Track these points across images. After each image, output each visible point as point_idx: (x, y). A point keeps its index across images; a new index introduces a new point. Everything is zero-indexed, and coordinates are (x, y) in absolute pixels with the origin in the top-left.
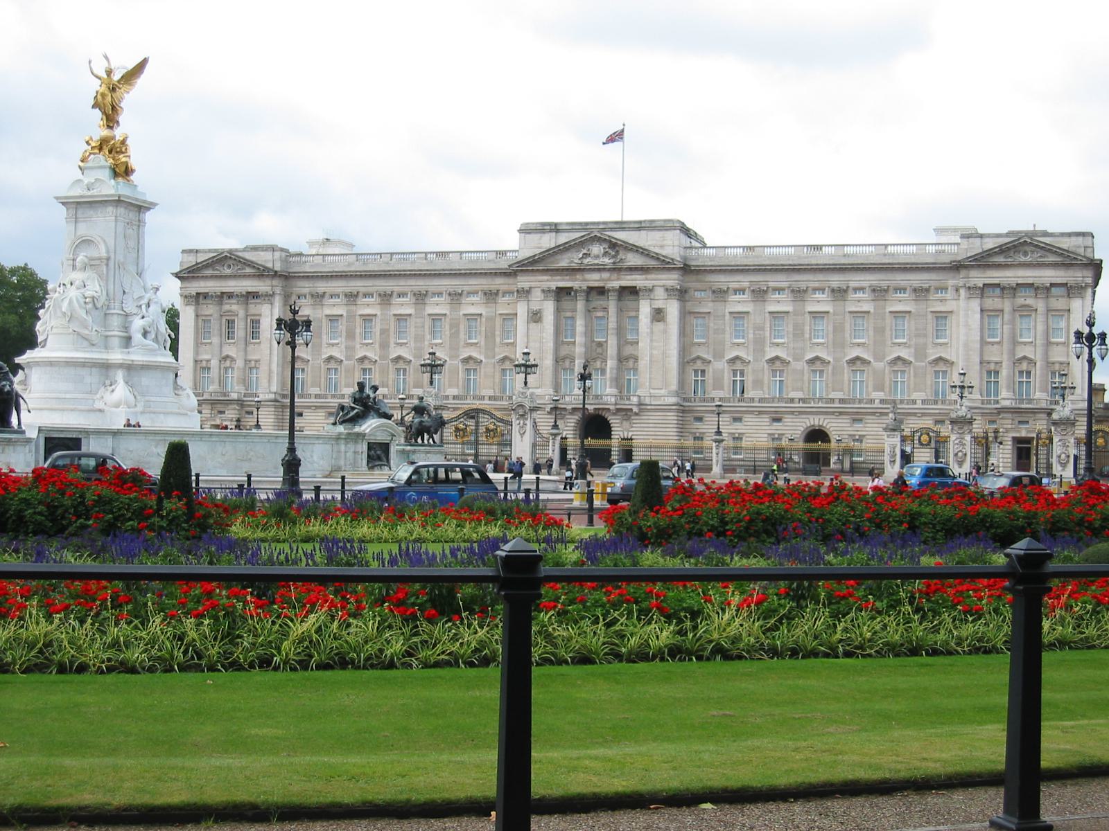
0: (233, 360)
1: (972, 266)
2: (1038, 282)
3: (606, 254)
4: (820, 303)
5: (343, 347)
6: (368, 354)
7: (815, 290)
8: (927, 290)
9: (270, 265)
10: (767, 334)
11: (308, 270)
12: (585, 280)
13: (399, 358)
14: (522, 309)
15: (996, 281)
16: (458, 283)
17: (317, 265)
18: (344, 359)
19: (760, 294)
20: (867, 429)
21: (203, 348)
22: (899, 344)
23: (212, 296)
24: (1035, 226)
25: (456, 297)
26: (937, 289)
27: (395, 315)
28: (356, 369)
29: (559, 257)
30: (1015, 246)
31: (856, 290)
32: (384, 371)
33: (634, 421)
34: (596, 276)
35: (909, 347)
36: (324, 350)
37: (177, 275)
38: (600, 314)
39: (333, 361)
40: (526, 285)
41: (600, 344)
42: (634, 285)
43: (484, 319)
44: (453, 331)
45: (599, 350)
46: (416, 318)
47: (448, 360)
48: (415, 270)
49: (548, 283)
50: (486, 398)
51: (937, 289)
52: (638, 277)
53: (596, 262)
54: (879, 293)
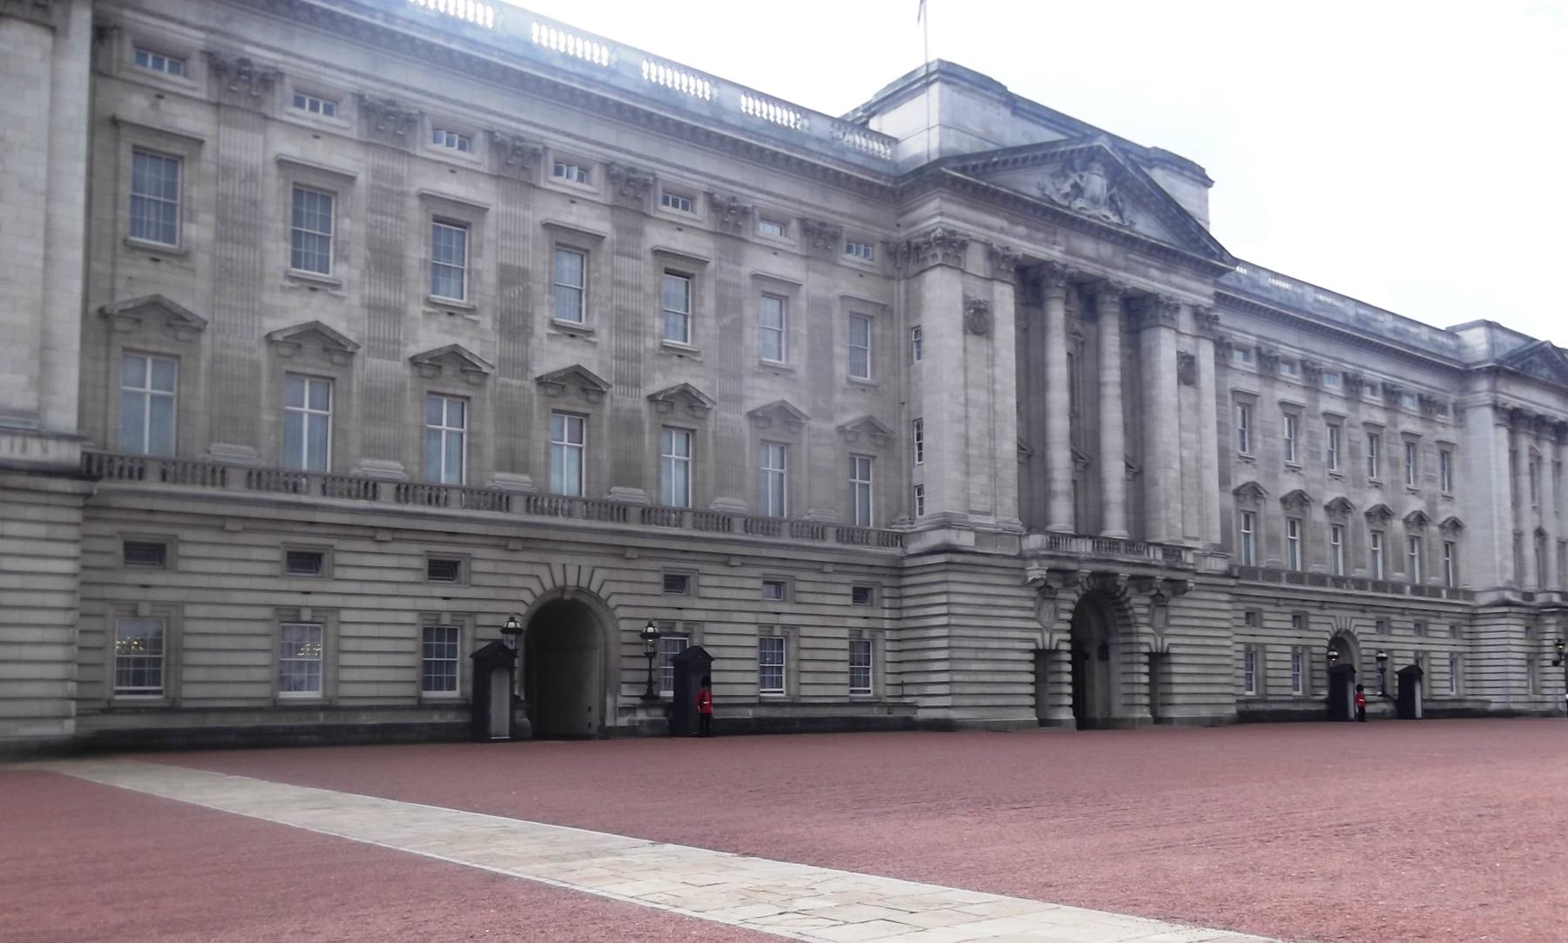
3: (1112, 201)
5: (354, 299)
6: (463, 342)
10: (1280, 446)
12: (1068, 252)
15: (1516, 403)
19: (1268, 363)
25: (731, 218)
27: (548, 226)
28: (409, 394)
32: (512, 418)
34: (1088, 246)
35: (1420, 497)
36: (267, 298)
39: (311, 347)
43: (803, 304)
44: (726, 320)
46: (619, 253)
49: (1002, 237)
50: (831, 532)
52: (1154, 272)
54: (1392, 394)
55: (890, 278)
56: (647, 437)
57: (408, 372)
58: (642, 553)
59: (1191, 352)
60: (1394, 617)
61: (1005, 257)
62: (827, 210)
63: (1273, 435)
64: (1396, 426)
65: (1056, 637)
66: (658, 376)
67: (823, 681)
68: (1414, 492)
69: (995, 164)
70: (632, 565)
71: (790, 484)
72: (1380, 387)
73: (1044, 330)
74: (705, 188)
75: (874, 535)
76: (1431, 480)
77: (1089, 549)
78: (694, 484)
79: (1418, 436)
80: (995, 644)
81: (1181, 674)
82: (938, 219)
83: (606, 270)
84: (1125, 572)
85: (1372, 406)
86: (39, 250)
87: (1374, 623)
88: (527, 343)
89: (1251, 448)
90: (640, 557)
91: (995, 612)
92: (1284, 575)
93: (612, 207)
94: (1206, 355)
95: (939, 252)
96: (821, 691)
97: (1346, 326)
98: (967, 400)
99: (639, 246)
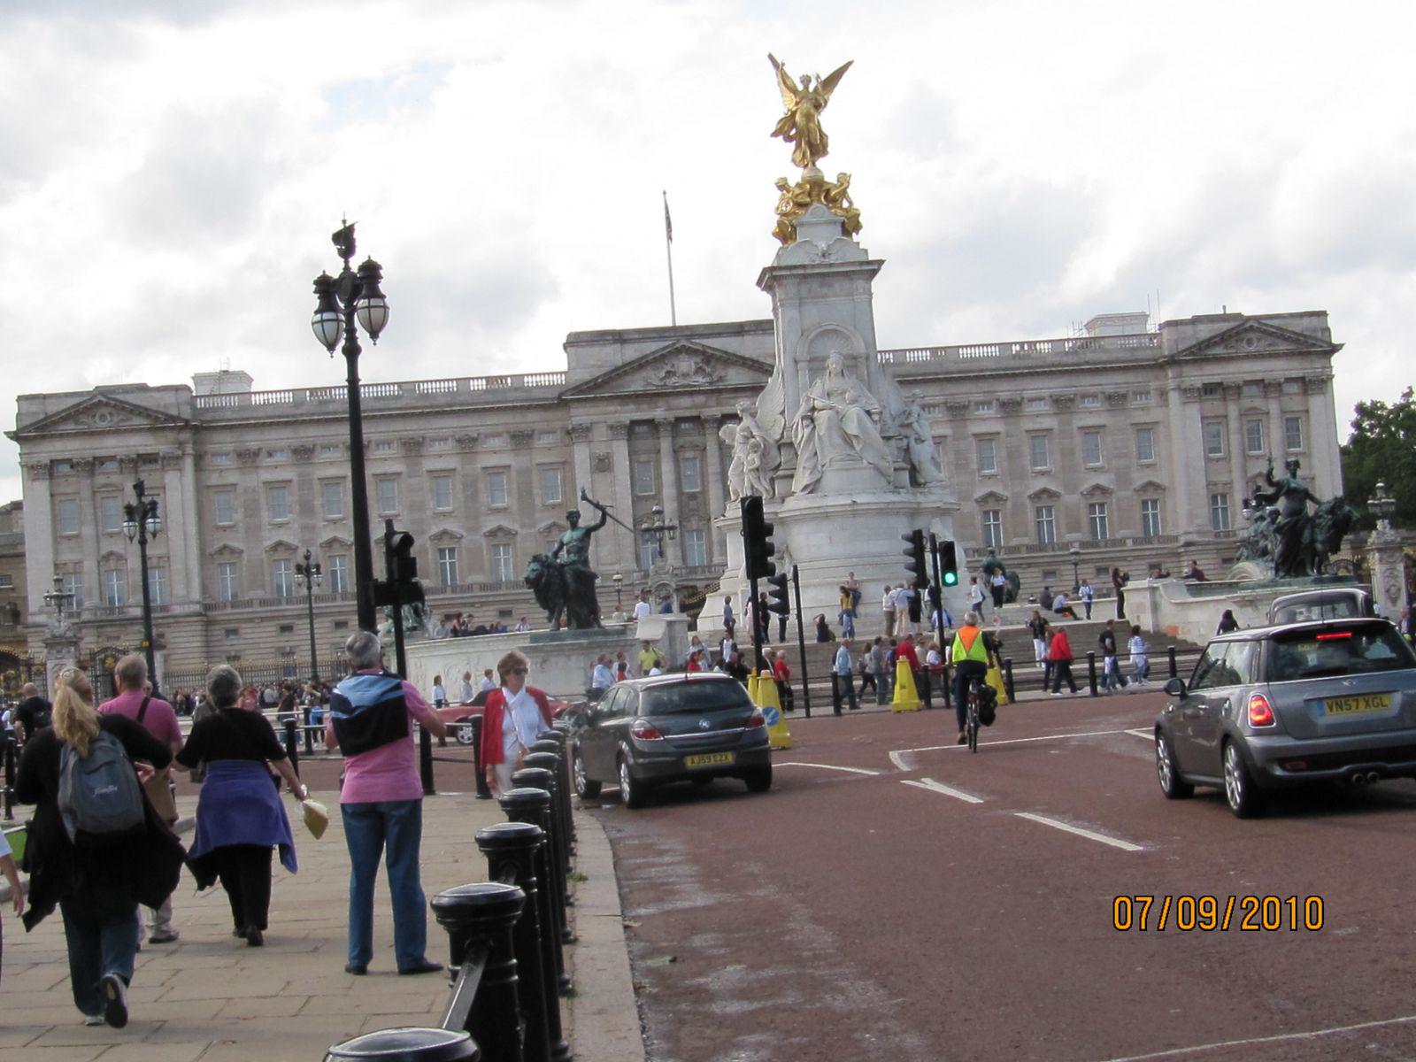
0: (120, 557)
1: (1187, 362)
2: (1268, 377)
3: (699, 370)
4: (987, 421)
5: (296, 526)
6: (339, 535)
7: (978, 404)
8: (1124, 396)
9: (174, 412)
11: (229, 415)
12: (669, 409)
14: (581, 455)
15: (1217, 379)
16: (470, 424)
17: (241, 408)
18: (299, 545)
21: (65, 545)
22: (1095, 470)
23: (78, 463)
24: (1224, 307)
25: (467, 444)
26: (1135, 394)
29: (628, 378)
30: (1238, 333)
31: (1032, 400)
34: (685, 401)
35: (1107, 471)
37: (15, 436)
38: (689, 454)
41: (693, 496)
43: (513, 473)
45: (693, 504)
46: (410, 477)
47: (465, 534)
48: (406, 409)
51: (1135, 394)
53: (685, 382)
54: (1062, 404)
55: (568, 445)
57: (319, 550)
60: (1062, 567)
79: (1104, 426)
84: (699, 584)
86: (182, 543)
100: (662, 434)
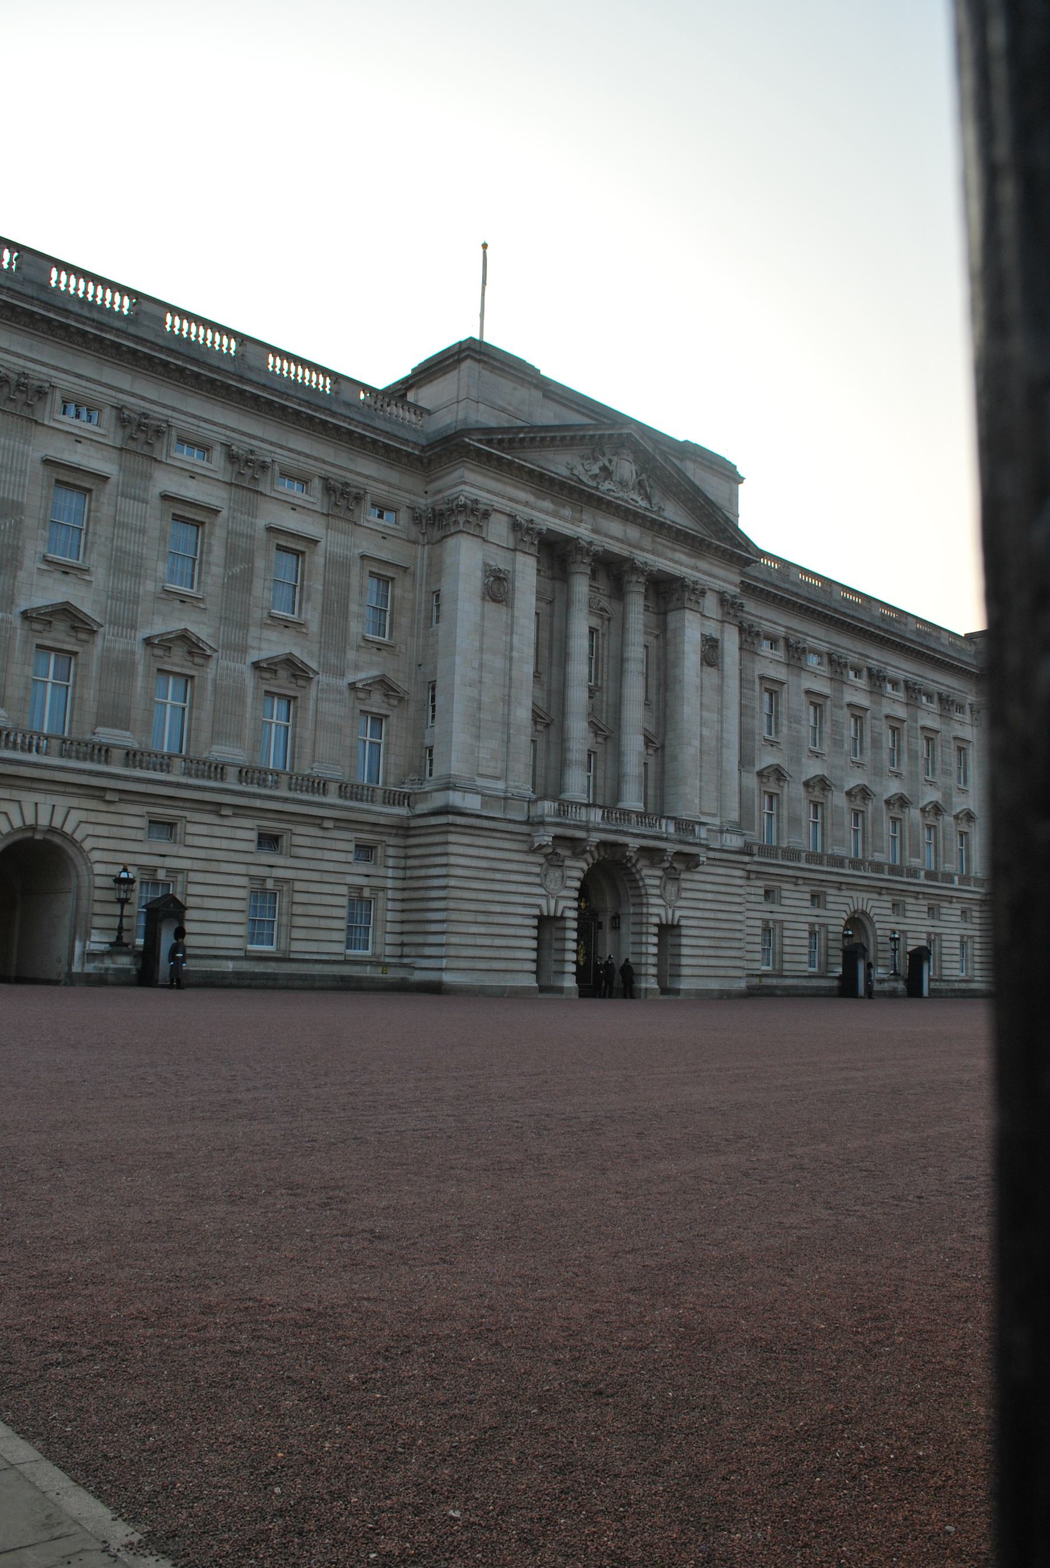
8: (953, 702)
10: (805, 732)
12: (595, 531)
13: (66, 612)
14: (467, 558)
16: (260, 435)
19: (795, 653)
20: (908, 921)
25: (247, 469)
27: (47, 462)
33: (684, 885)
34: (615, 527)
35: (937, 789)
40: (483, 496)
42: (677, 573)
43: (322, 561)
44: (237, 570)
49: (527, 510)
50: (333, 787)
55: (415, 543)
56: (139, 682)
58: (124, 797)
59: (716, 635)
60: (909, 900)
61: (528, 529)
62: (351, 471)
63: (799, 722)
64: (916, 721)
65: (562, 904)
66: (158, 620)
67: (318, 938)
68: (931, 784)
69: (522, 440)
70: (112, 808)
71: (294, 738)
72: (902, 684)
73: (568, 605)
74: (223, 439)
75: (380, 793)
76: (946, 773)
77: (599, 819)
78: (189, 730)
80: (498, 908)
81: (689, 945)
82: (463, 487)
83: (106, 511)
85: (894, 701)
87: (890, 905)
88: (15, 577)
89: (777, 732)
90: (121, 800)
91: (498, 876)
92: (803, 855)
93: (121, 449)
94: (731, 641)
95: (461, 519)
96: (313, 947)
97: (869, 624)
98: (481, 665)
99: (146, 490)
100: (575, 568)
